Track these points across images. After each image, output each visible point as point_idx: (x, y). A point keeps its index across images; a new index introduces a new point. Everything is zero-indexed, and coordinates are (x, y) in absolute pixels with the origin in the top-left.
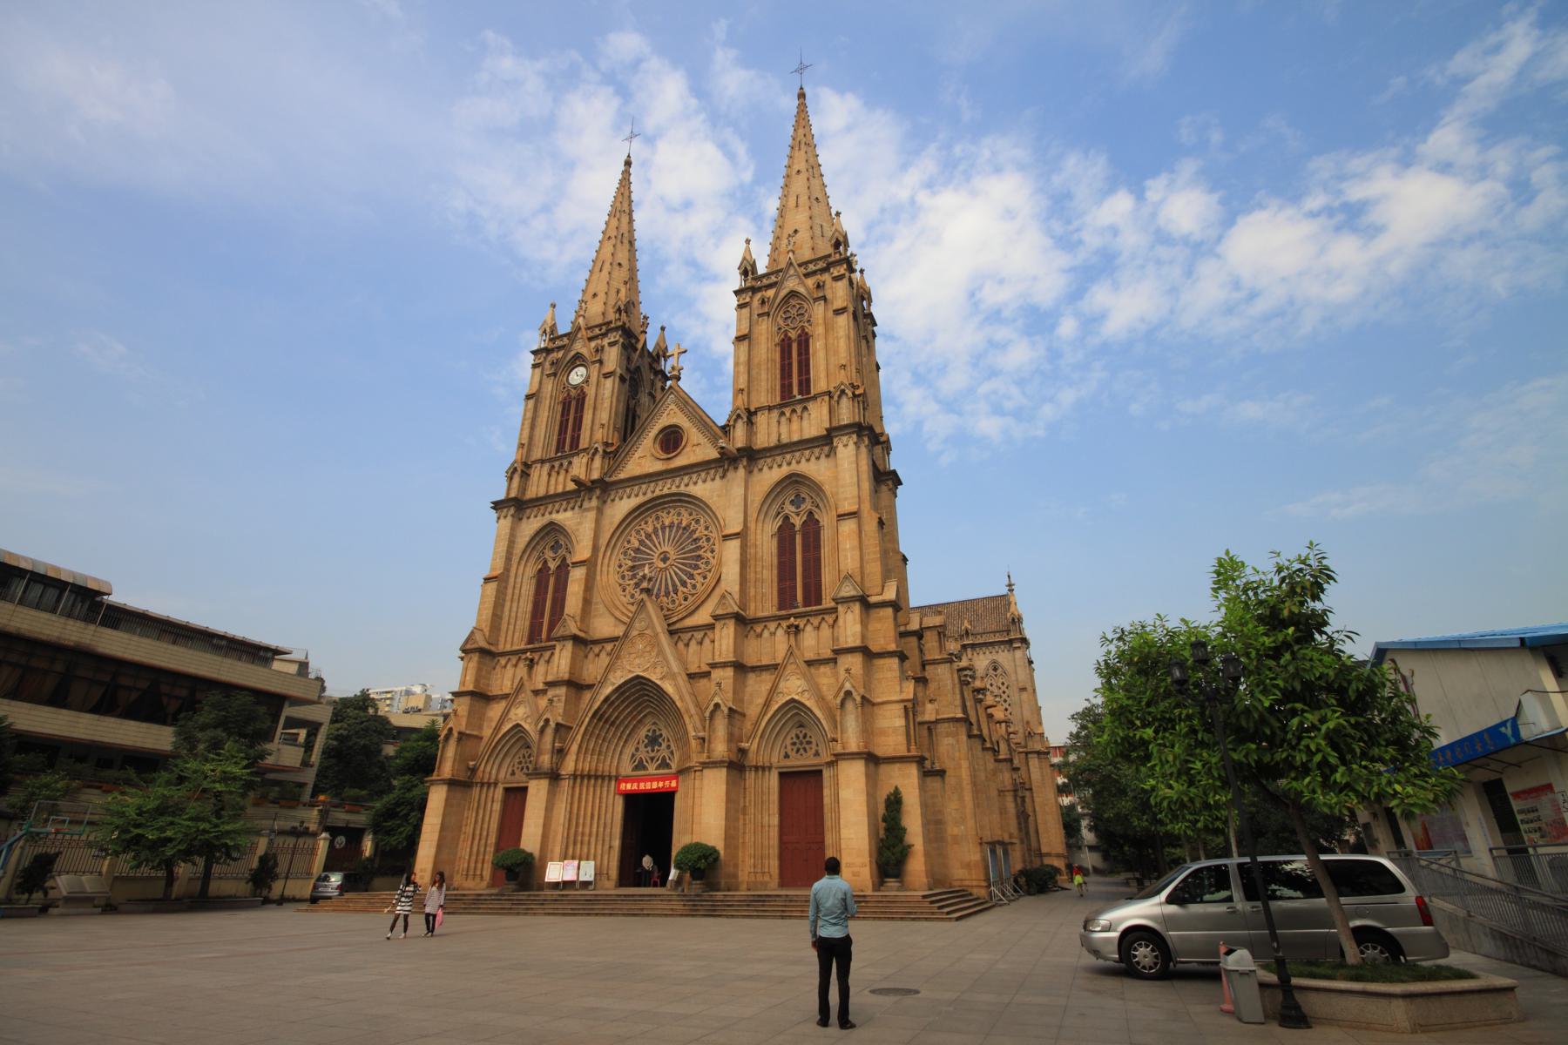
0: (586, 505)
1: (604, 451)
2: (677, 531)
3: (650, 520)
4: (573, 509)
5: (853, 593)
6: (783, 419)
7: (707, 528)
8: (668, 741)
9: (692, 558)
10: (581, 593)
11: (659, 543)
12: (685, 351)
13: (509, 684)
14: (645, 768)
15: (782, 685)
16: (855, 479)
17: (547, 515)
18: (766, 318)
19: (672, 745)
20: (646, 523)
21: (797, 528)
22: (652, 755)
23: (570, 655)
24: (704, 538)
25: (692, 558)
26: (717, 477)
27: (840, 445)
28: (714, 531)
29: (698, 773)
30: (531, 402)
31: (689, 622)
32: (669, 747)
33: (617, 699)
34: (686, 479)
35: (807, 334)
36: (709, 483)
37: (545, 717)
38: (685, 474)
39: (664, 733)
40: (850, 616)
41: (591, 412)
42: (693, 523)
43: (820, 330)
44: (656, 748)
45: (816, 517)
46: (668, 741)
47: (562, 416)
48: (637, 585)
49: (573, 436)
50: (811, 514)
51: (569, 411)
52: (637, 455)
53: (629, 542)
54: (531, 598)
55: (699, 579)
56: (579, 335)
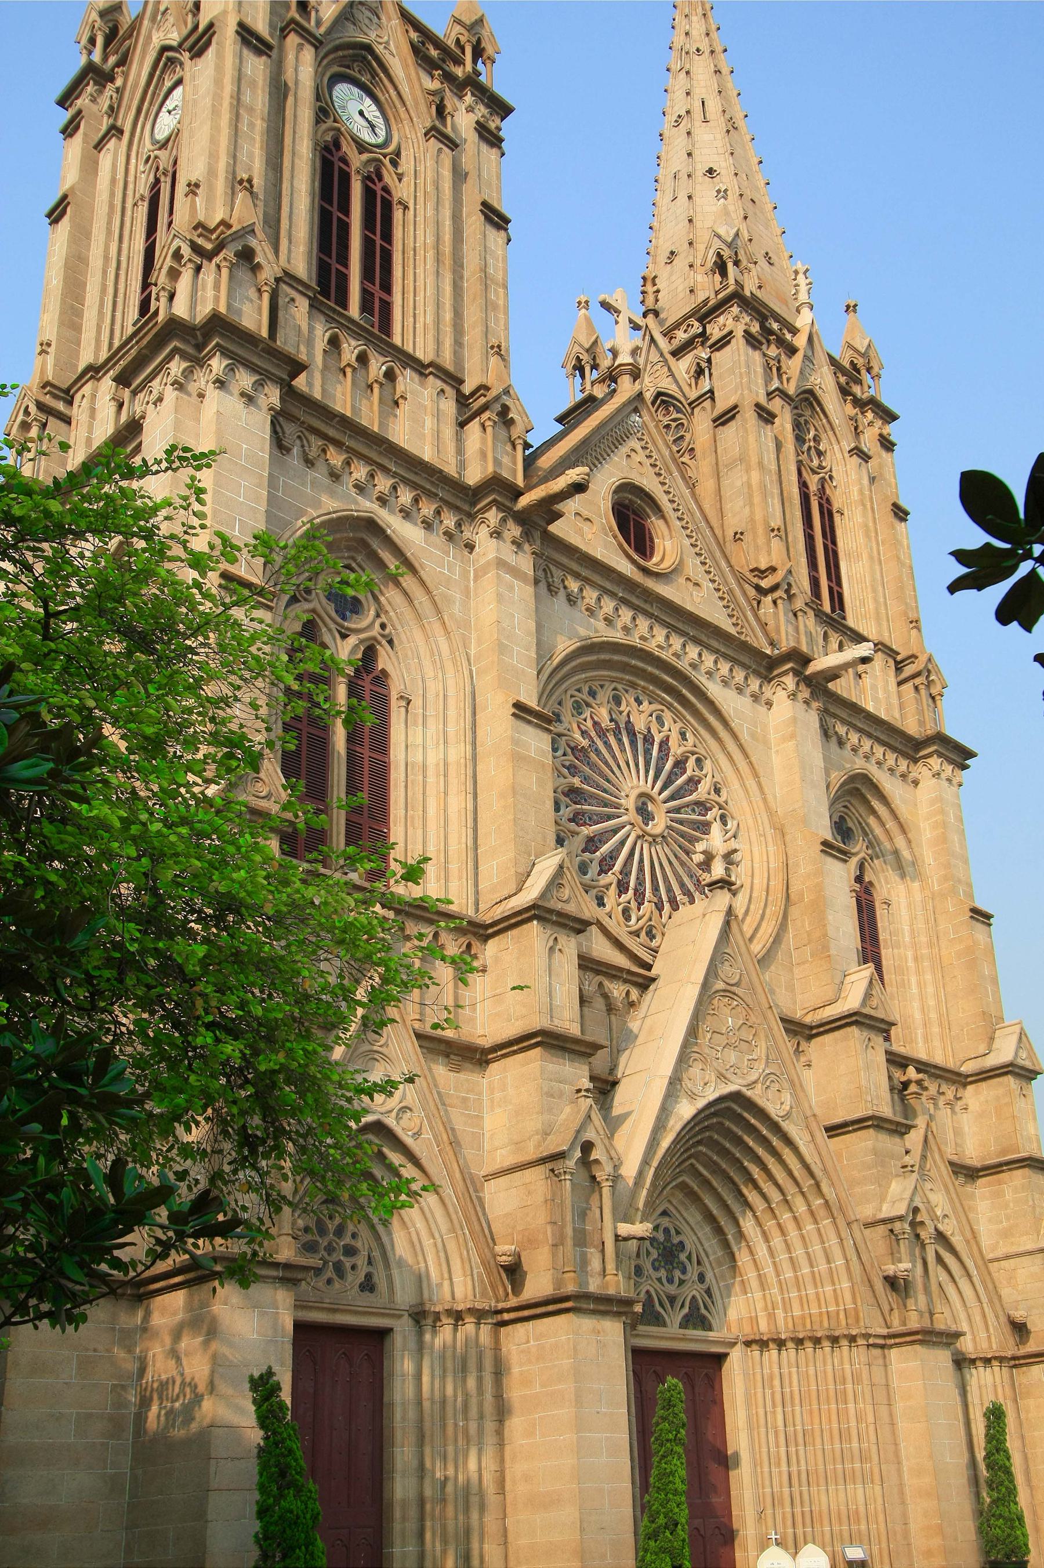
8: (699, 1263)
14: (658, 1320)
19: (709, 1276)
22: (672, 1289)
32: (702, 1278)
44: (677, 1274)
46: (699, 1263)
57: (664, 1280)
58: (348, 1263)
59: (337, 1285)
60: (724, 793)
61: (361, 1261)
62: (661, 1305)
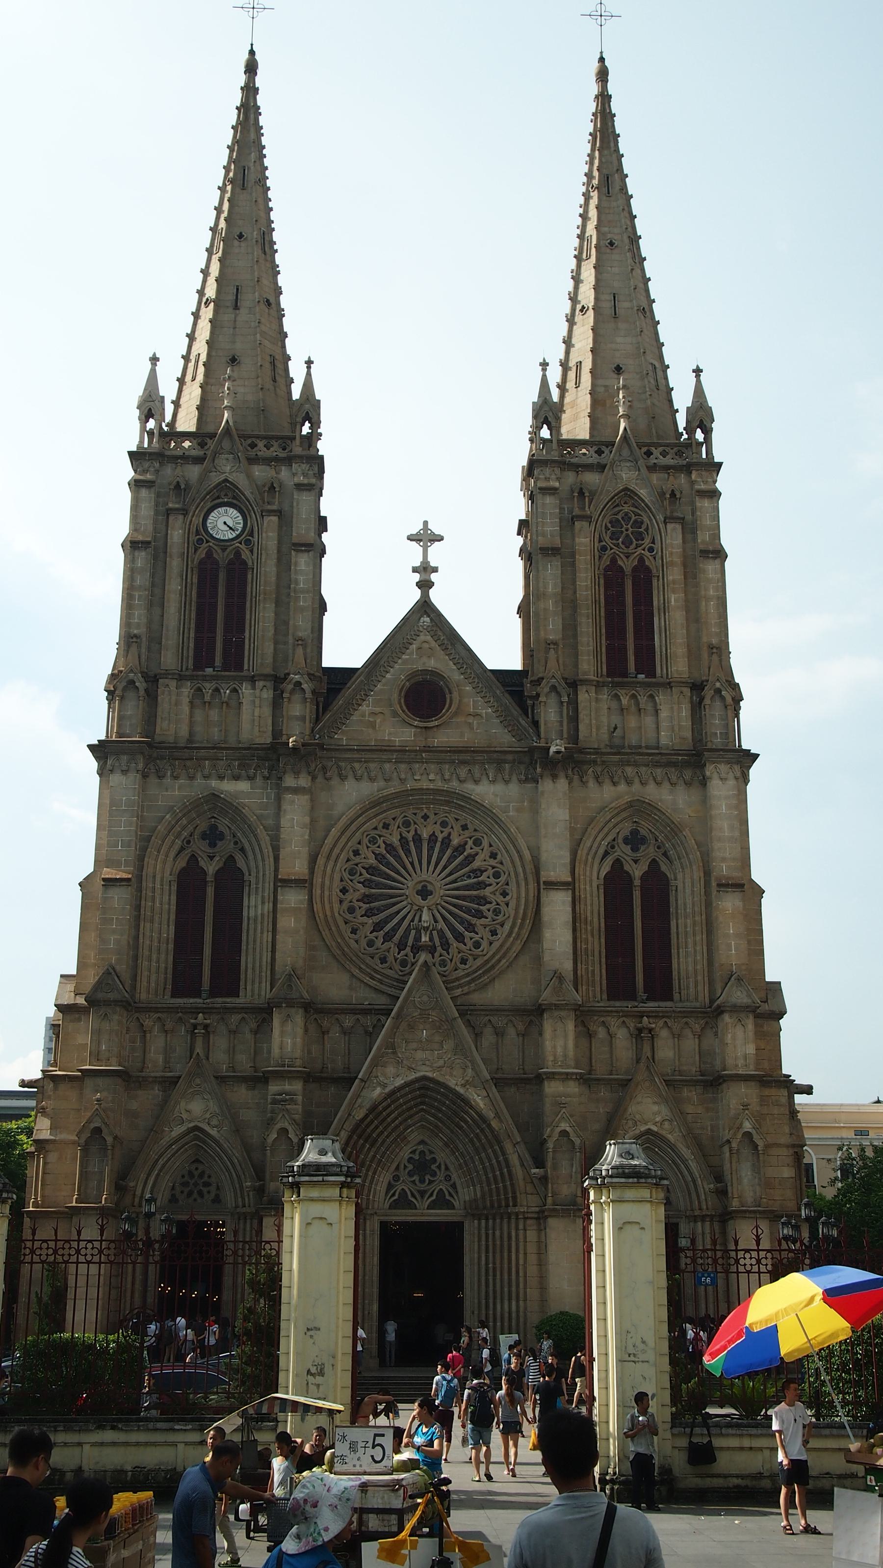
0: (289, 781)
1: (313, 692)
2: (442, 852)
3: (393, 827)
4: (250, 778)
5: (746, 1001)
6: (614, 705)
7: (493, 856)
9: (471, 899)
10: (302, 932)
11: (412, 864)
12: (440, 539)
13: (161, 1059)
15: (633, 1109)
16: (737, 834)
17: (199, 781)
18: (585, 524)
19: (454, 1177)
20: (386, 826)
21: (637, 882)
22: (423, 1187)
23: (300, 1031)
24: (491, 872)
25: (471, 899)
26: (514, 778)
27: (715, 775)
28: (507, 861)
29: (529, 1222)
30: (142, 557)
31: (477, 998)
32: (448, 1178)
33: (385, 1109)
34: (463, 772)
35: (648, 570)
36: (499, 788)
37: (278, 1126)
38: (463, 762)
39: (442, 1156)
40: (739, 1032)
41: (270, 606)
42: (470, 842)
43: (675, 574)
44: (427, 1177)
45: (664, 868)
46: (447, 1168)
47: (200, 595)
48: (377, 927)
49: (226, 642)
50: (654, 863)
51: (215, 587)
52: (364, 708)
53: (356, 853)
54: (173, 917)
55: (487, 935)
56: (226, 444)
57: (417, 1183)
58: (205, 1190)
59: (199, 1201)
60: (499, 857)
61: (213, 1189)
62: (413, 1195)
